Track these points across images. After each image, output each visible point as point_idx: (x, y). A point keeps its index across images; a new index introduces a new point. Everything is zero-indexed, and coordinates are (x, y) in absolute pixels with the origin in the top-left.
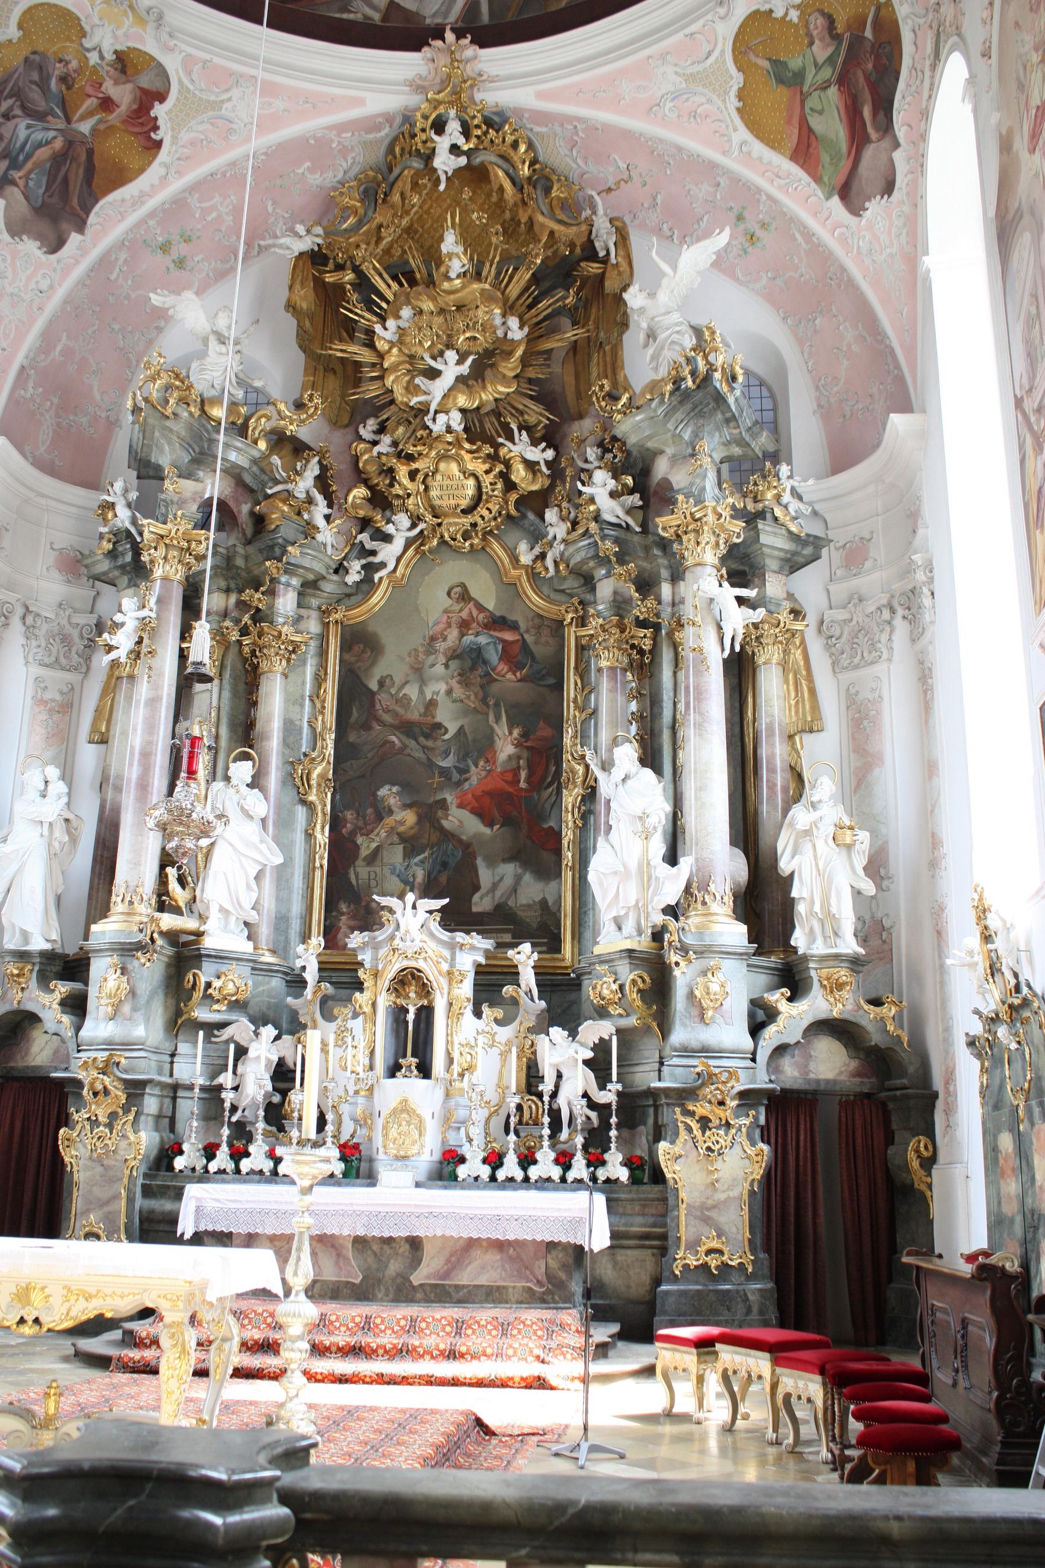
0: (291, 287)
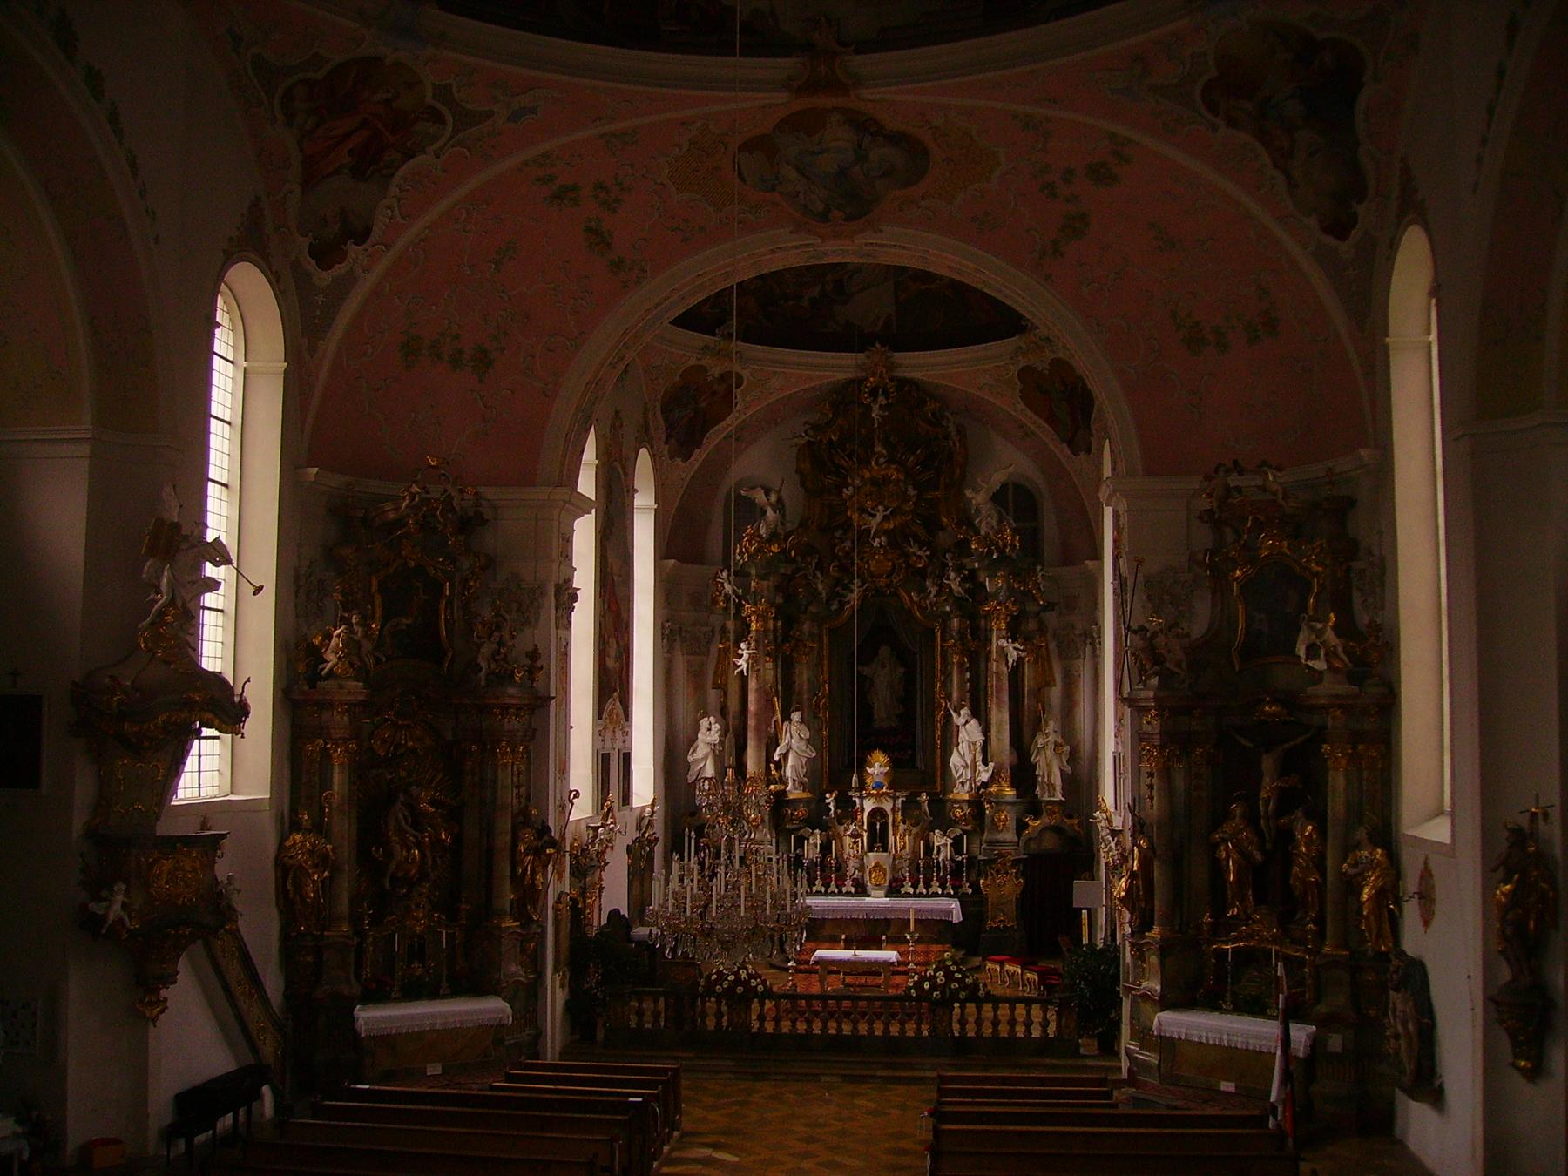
0: (798, 460)
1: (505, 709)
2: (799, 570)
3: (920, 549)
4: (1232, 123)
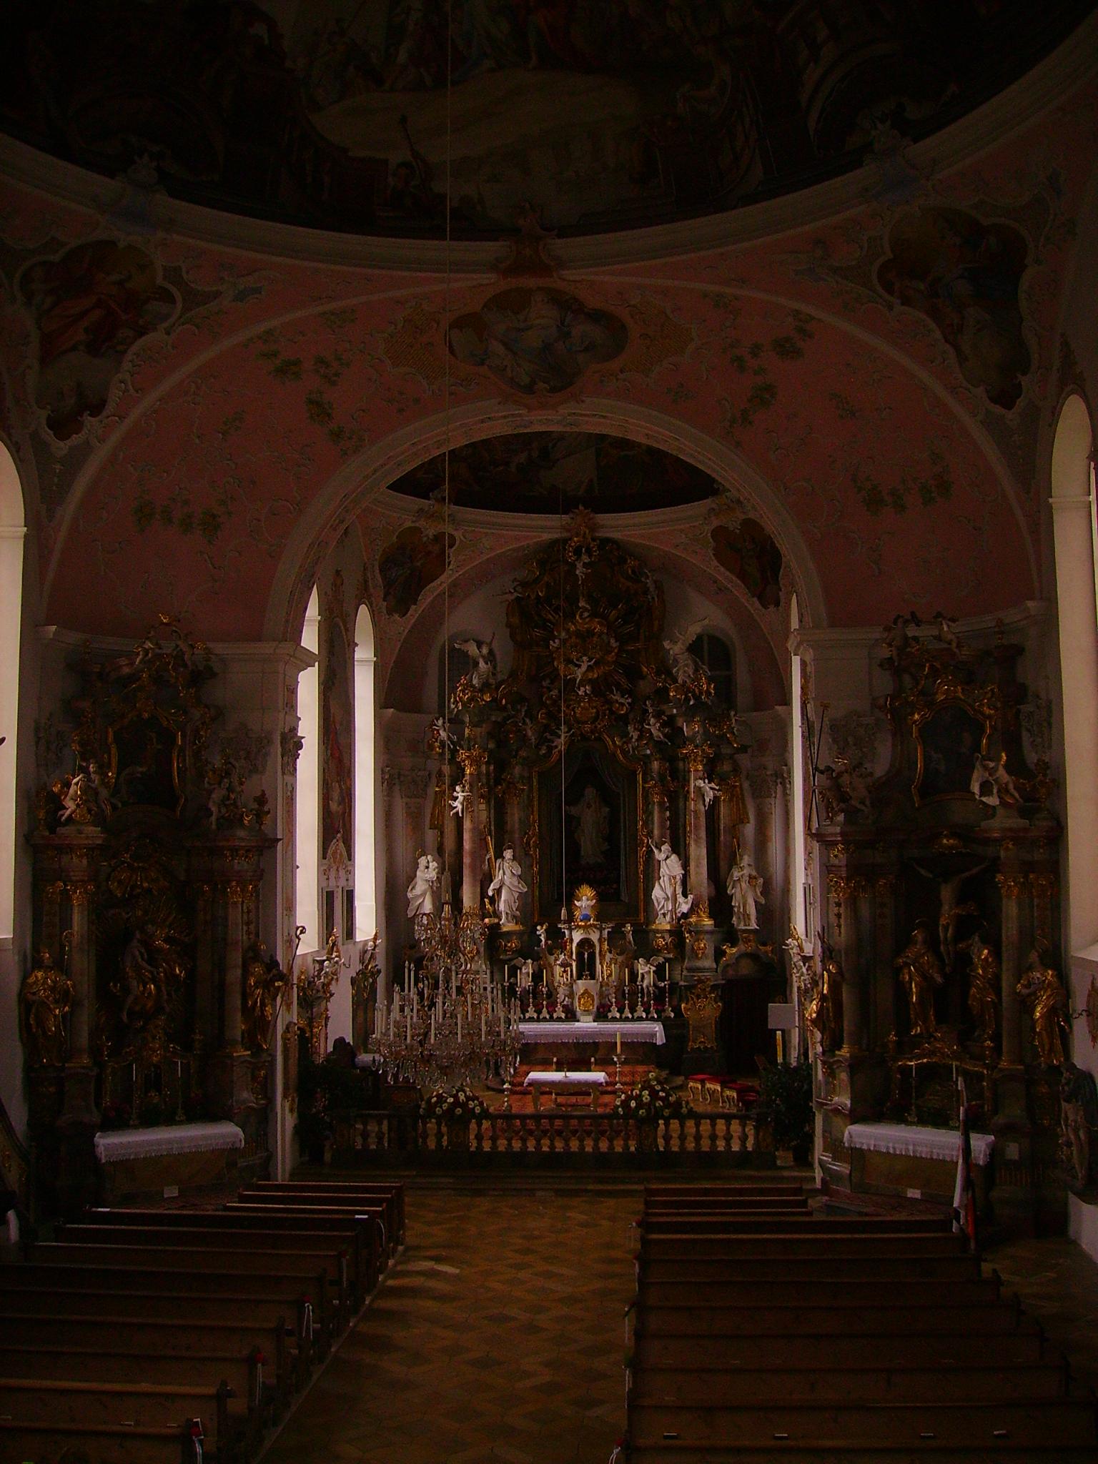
1: (234, 851)
2: (509, 717)
3: (623, 697)
4: (906, 301)
